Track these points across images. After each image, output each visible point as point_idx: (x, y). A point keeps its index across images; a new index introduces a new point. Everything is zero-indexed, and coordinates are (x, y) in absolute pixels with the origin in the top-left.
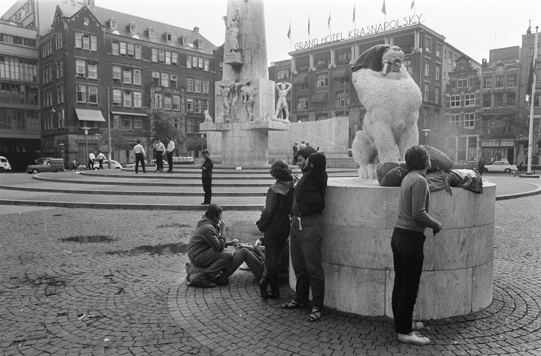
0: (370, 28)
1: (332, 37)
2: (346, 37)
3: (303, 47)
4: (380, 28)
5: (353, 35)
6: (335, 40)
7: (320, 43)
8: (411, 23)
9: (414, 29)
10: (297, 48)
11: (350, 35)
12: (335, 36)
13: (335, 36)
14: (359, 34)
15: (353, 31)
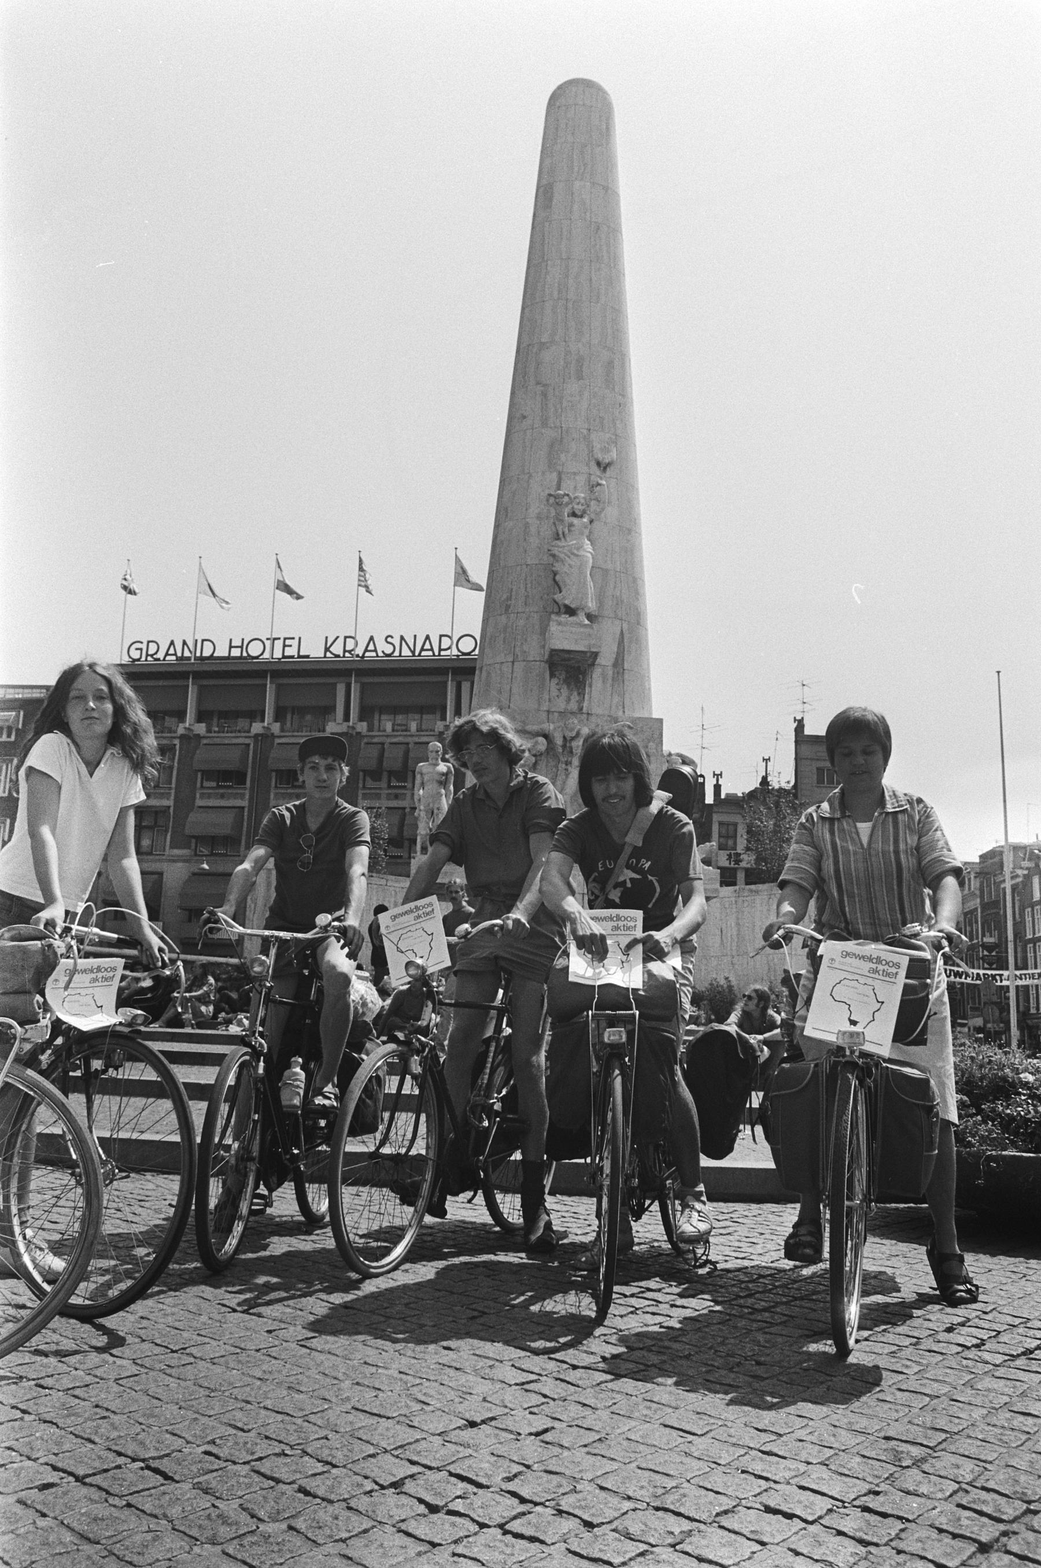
0: (396, 641)
1: (268, 643)
2: (314, 650)
3: (161, 655)
4: (428, 646)
5: (338, 649)
6: (278, 654)
7: (222, 652)
8: (328, 654)
9: (265, 672)
10: (135, 655)
11: (327, 649)
12: (278, 644)
13: (278, 644)
14: (359, 651)
15: (341, 640)
